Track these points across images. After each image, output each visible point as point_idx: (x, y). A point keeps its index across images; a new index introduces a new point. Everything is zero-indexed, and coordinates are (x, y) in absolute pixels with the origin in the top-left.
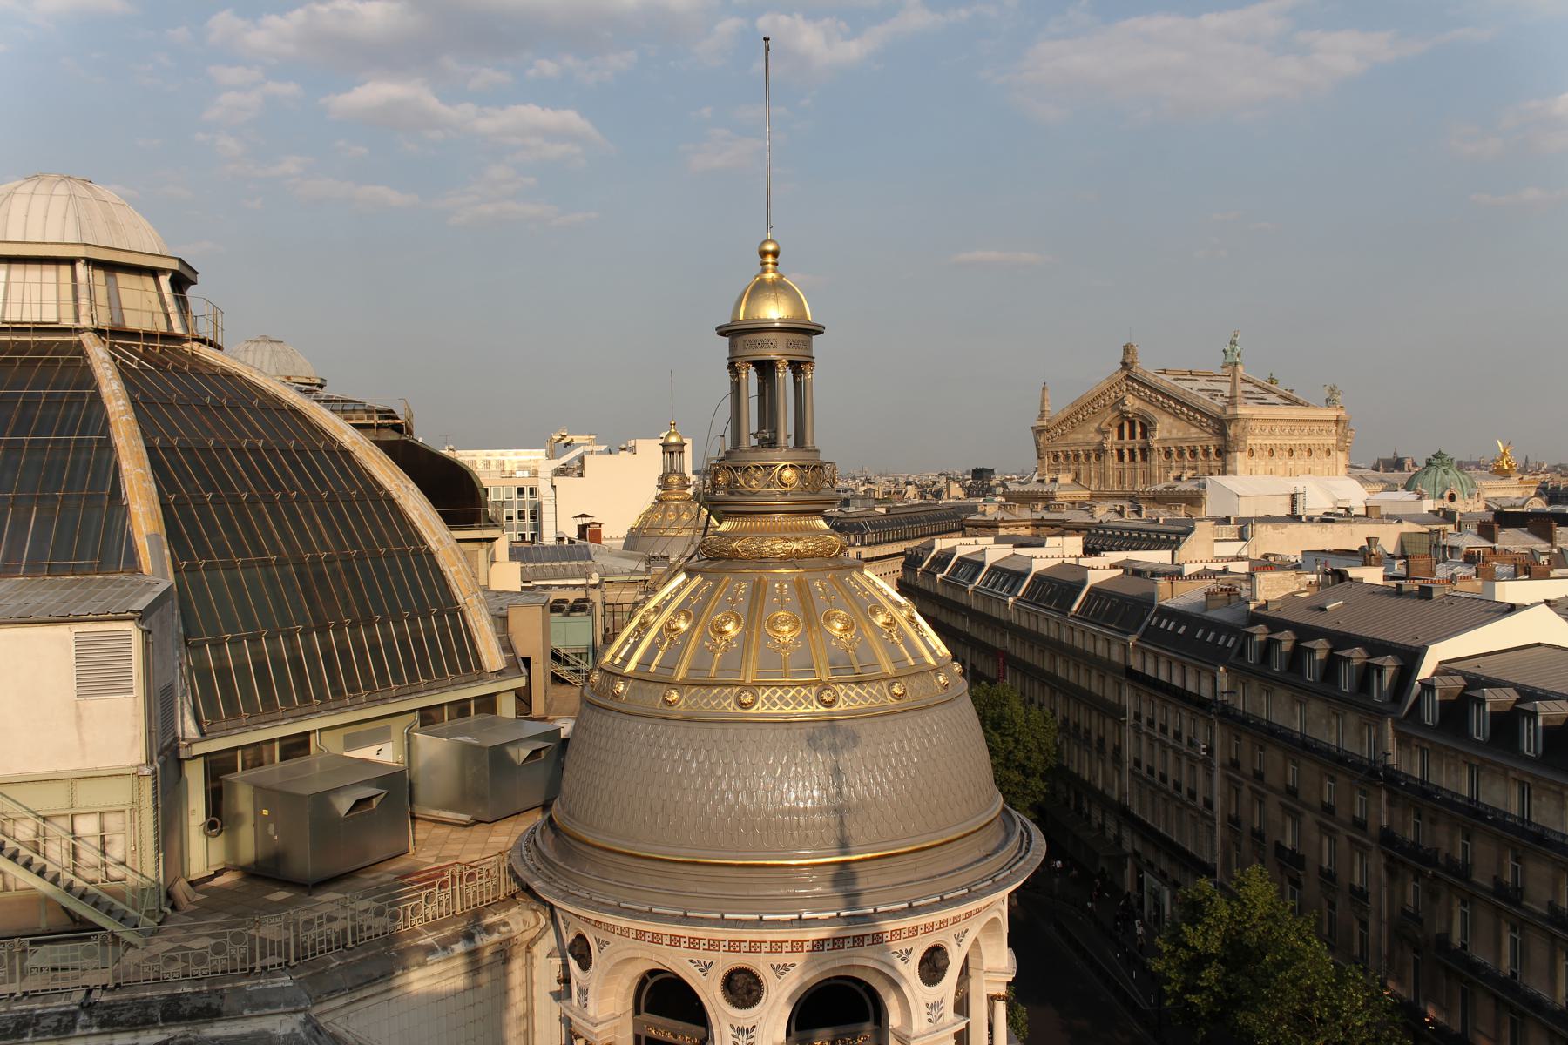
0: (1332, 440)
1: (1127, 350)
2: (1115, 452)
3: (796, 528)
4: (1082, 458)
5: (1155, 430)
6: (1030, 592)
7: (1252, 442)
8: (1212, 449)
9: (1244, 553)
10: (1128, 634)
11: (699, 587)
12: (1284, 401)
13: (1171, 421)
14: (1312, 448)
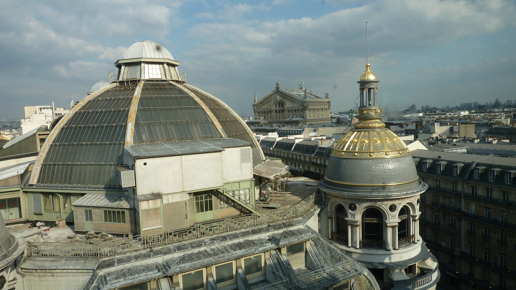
0: (327, 107)
1: (277, 84)
4: (266, 113)
8: (300, 110)
10: (312, 154)
11: (356, 135)
13: (289, 102)
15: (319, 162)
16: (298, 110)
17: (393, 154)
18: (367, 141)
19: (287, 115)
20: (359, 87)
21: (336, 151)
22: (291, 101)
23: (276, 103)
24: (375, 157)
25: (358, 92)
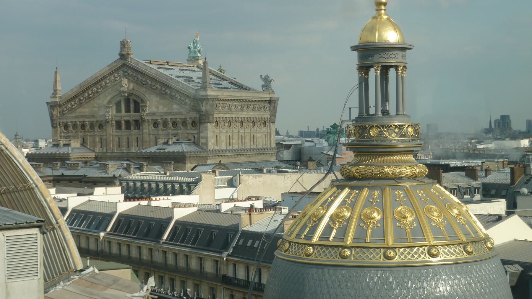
0: (267, 115)
1: (123, 44)
2: (114, 122)
3: (399, 160)
4: (88, 128)
5: (146, 106)
6: (114, 229)
7: (217, 116)
8: (189, 121)
9: (235, 196)
10: (221, 253)
11: (348, 196)
12: (234, 87)
13: (158, 99)
14: (231, 120)
15: (241, 275)
16: (184, 123)
17: (449, 252)
18: (377, 216)
19: (152, 136)
20: (357, 63)
21: (290, 242)
22: (162, 95)
23: (118, 99)
24: (399, 260)
25: (355, 76)
